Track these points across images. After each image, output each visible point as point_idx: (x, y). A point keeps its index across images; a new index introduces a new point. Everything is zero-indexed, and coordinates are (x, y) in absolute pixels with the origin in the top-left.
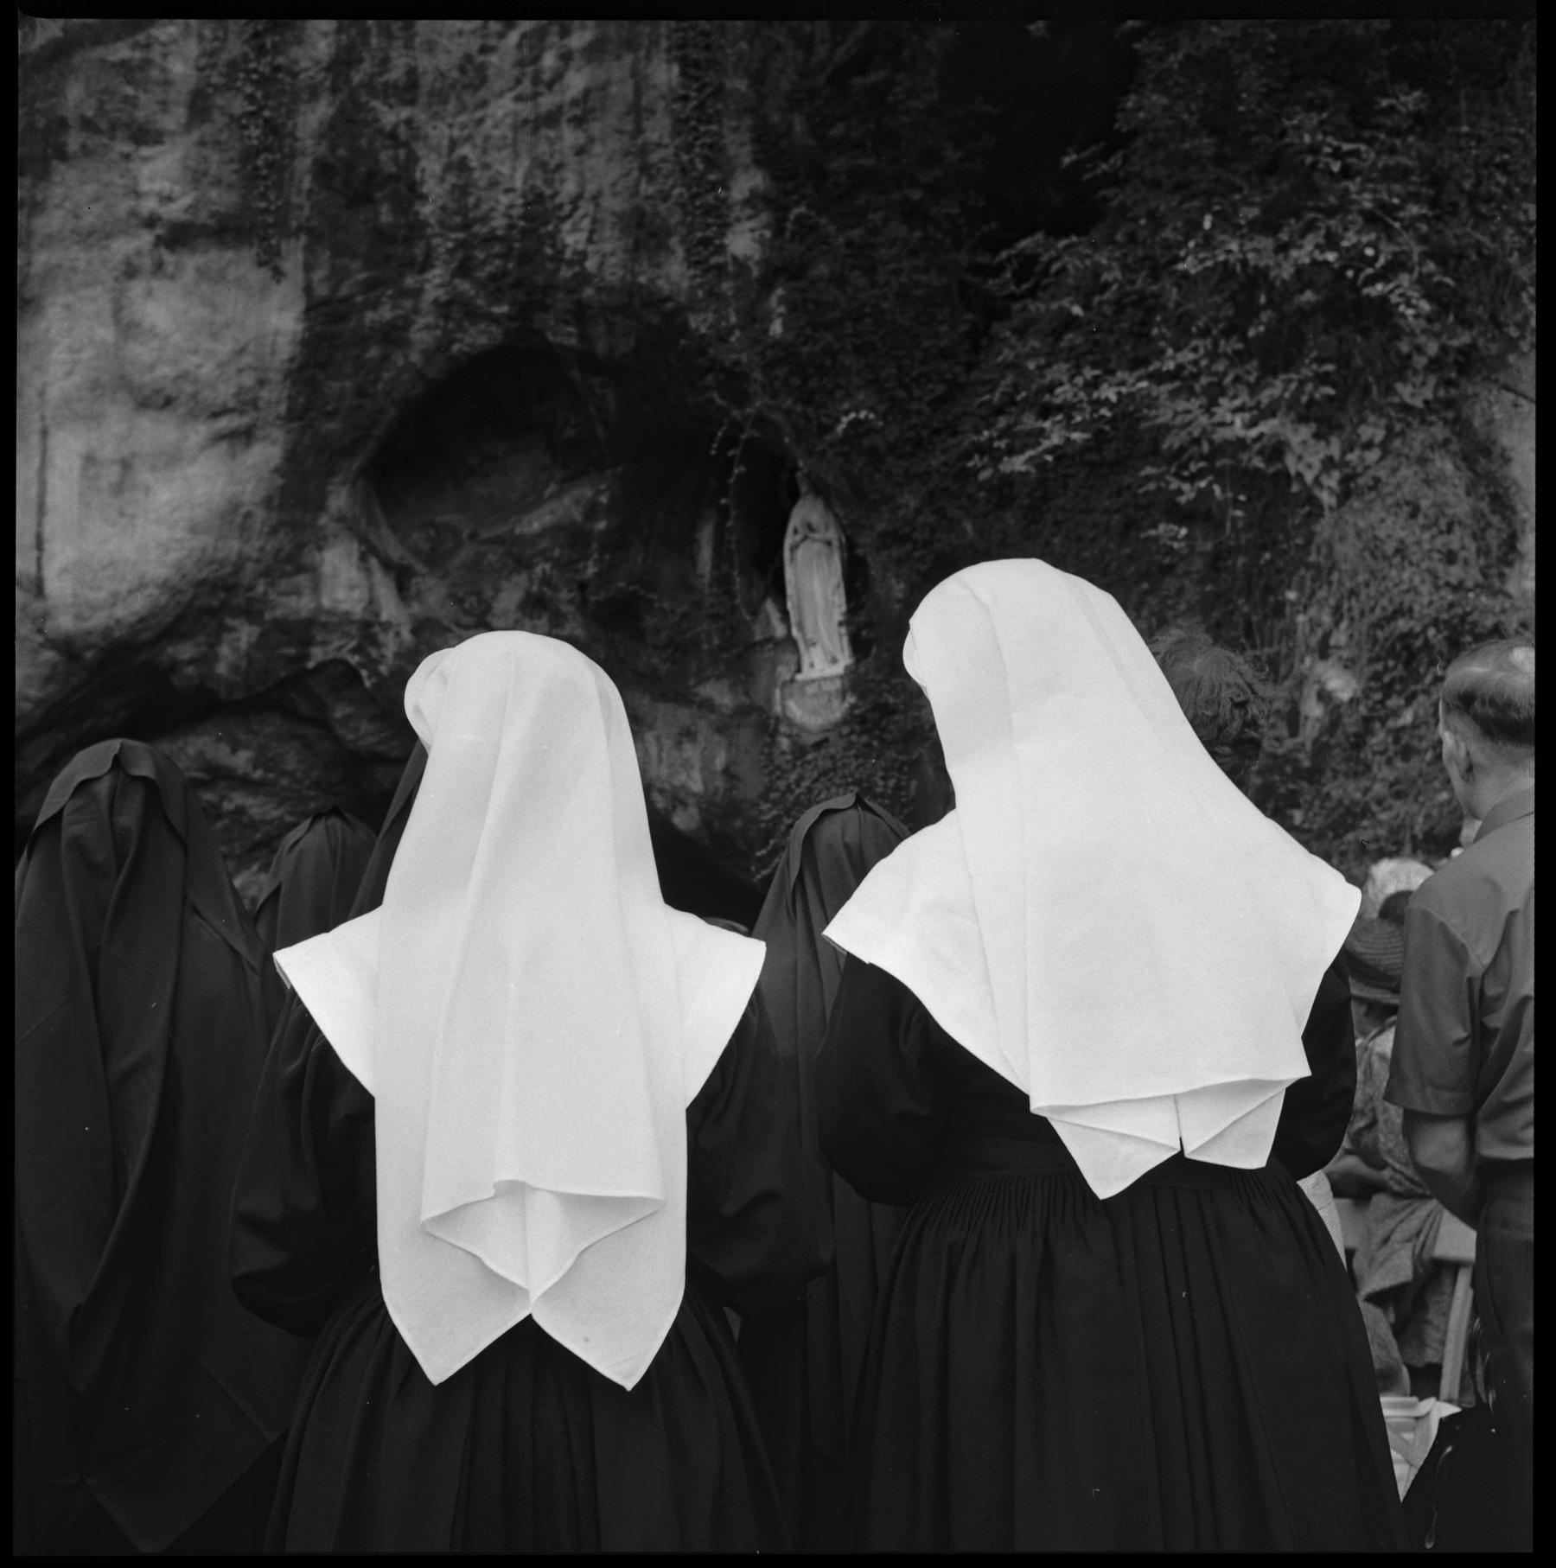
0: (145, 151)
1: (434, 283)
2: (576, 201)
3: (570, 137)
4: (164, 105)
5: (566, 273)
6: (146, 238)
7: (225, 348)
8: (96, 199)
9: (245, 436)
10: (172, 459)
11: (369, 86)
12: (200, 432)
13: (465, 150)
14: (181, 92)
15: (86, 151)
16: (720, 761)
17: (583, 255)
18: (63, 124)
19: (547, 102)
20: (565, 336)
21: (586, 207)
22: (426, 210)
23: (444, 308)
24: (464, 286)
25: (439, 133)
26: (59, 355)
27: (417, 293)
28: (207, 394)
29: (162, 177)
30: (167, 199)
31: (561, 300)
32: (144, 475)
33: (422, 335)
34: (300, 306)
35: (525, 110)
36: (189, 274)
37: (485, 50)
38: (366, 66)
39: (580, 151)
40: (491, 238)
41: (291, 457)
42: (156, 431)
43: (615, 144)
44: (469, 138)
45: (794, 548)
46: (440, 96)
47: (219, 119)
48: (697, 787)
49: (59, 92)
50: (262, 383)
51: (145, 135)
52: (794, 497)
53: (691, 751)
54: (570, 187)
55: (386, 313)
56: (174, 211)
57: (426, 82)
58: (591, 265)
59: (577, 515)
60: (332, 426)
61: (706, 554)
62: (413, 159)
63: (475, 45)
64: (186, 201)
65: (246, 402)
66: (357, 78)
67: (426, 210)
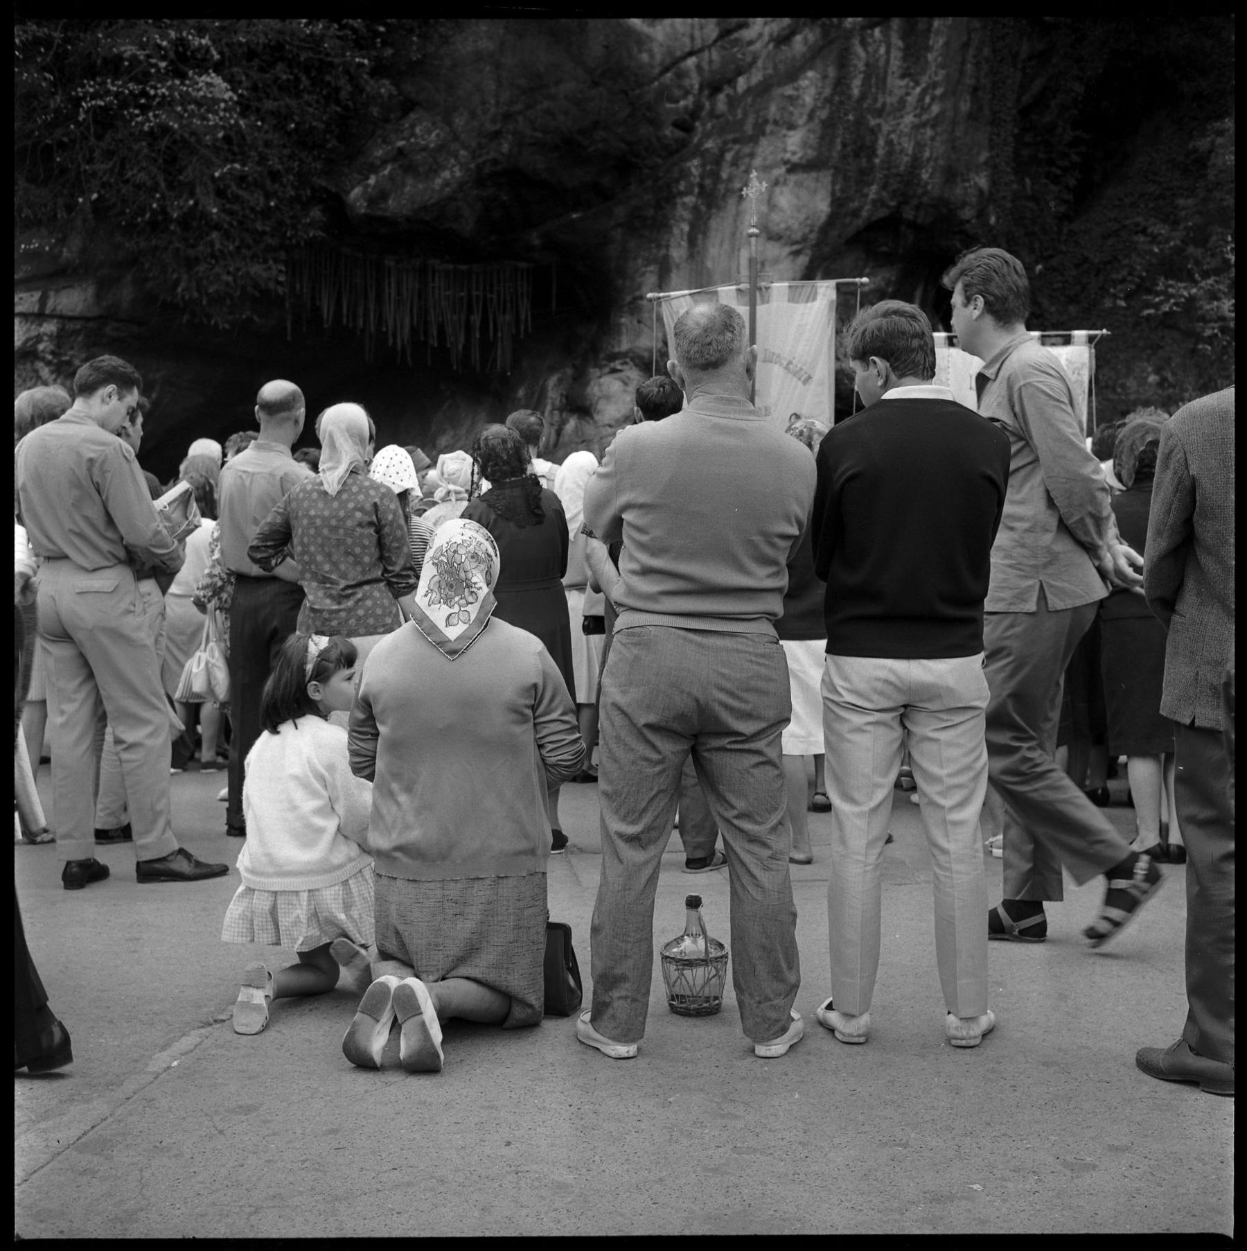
0: (791, 133)
2: (929, 160)
3: (929, 132)
4: (801, 114)
5: (920, 191)
6: (783, 169)
7: (802, 217)
8: (772, 153)
9: (796, 253)
10: (776, 261)
12: (787, 250)
13: (893, 136)
15: (772, 133)
17: (927, 183)
18: (766, 121)
19: (925, 117)
20: (908, 214)
21: (932, 163)
22: (877, 161)
23: (874, 202)
24: (884, 194)
25: (886, 128)
27: (866, 195)
28: (793, 236)
29: (795, 143)
30: (794, 153)
31: (915, 202)
32: (767, 268)
33: (864, 214)
34: (829, 200)
35: (916, 120)
36: (791, 184)
37: (908, 94)
38: (869, 101)
39: (933, 139)
41: (811, 262)
42: (773, 250)
46: (889, 114)
47: (817, 121)
49: (767, 108)
50: (811, 231)
51: (792, 127)
54: (927, 154)
55: (856, 204)
56: (795, 159)
57: (888, 108)
58: (929, 187)
59: (883, 284)
62: (876, 140)
63: (903, 91)
64: (799, 155)
65: (804, 239)
66: (865, 105)
67: (877, 161)
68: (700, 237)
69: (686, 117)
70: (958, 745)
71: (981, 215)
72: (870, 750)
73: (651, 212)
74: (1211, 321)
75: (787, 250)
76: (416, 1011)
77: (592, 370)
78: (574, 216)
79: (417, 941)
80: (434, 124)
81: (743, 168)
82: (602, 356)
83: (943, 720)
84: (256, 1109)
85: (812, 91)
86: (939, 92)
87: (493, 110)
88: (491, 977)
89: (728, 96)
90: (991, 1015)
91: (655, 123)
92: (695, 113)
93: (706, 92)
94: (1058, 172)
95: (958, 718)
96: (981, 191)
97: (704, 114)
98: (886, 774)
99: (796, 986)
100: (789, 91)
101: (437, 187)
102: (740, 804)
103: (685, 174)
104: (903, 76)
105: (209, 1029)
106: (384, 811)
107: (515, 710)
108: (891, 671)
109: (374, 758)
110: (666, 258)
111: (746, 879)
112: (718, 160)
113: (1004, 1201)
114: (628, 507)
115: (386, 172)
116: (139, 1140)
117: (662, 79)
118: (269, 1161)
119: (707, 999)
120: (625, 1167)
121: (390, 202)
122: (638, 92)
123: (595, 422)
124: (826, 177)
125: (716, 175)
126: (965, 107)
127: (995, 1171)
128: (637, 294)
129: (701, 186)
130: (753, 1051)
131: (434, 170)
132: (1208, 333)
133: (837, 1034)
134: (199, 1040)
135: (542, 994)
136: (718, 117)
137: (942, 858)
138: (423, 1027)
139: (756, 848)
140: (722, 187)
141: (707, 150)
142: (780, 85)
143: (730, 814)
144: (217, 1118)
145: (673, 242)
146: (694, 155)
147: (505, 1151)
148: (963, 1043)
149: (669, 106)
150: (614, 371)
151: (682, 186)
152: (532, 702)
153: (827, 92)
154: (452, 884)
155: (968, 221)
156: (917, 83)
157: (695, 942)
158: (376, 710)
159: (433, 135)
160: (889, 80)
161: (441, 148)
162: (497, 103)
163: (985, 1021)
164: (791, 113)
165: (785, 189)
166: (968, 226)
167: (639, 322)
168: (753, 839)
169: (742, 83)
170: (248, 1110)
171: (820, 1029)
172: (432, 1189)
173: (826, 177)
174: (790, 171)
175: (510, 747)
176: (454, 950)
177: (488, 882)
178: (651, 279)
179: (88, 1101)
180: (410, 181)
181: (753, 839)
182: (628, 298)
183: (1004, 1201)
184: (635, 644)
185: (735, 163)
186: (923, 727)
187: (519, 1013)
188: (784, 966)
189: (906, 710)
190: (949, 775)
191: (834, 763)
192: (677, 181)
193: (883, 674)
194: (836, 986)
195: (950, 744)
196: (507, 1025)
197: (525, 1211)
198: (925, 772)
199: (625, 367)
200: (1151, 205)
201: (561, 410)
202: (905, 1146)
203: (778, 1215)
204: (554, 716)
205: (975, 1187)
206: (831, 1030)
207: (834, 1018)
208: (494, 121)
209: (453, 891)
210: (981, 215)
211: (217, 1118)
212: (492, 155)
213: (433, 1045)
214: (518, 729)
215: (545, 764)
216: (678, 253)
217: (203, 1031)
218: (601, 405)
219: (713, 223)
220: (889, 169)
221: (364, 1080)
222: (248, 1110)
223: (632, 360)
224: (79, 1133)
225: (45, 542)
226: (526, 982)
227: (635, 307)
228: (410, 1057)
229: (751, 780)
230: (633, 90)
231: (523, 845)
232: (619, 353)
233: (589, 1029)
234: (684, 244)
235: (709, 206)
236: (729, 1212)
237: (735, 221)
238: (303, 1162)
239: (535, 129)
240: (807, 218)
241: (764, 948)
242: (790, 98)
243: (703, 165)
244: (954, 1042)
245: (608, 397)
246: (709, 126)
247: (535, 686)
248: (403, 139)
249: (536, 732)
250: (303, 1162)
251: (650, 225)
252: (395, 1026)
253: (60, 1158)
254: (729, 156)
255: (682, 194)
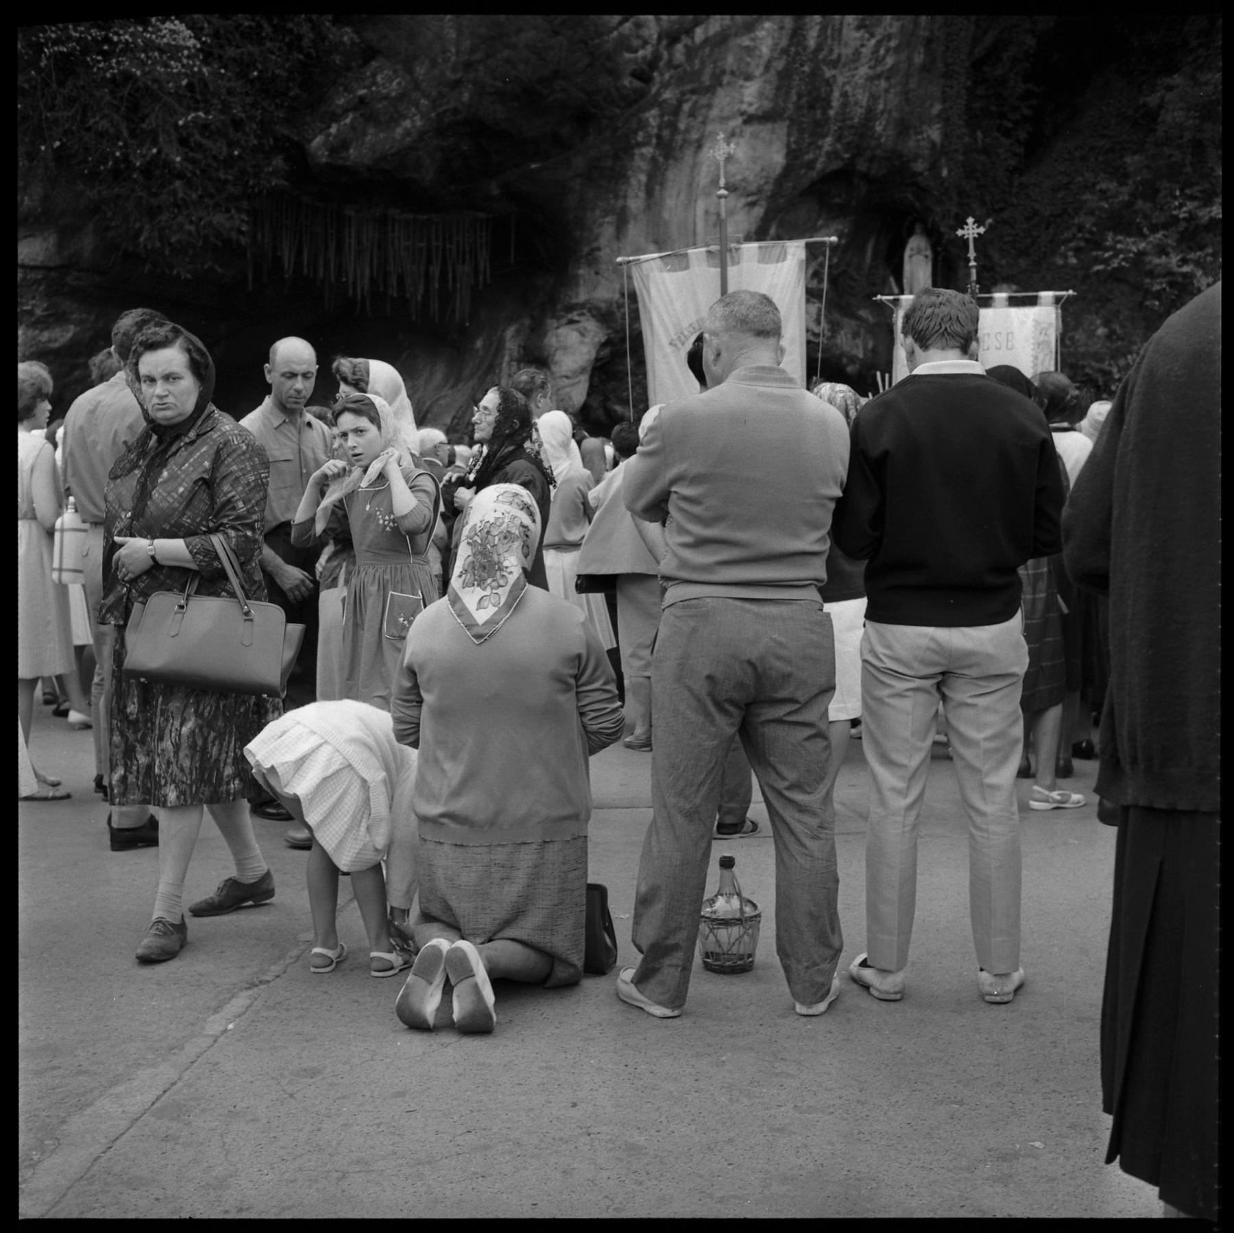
0: (748, 84)
1: (827, 143)
2: (883, 112)
3: (883, 84)
4: (758, 65)
5: (874, 143)
6: (739, 121)
7: (758, 168)
9: (752, 205)
11: (824, 61)
12: (743, 201)
13: (848, 88)
14: (763, 62)
15: (729, 84)
16: (870, 345)
18: (723, 72)
19: (879, 69)
20: (862, 166)
21: (886, 115)
23: (828, 154)
24: (839, 146)
25: (841, 80)
26: (704, 169)
27: (820, 148)
29: (751, 94)
30: (750, 104)
31: (868, 154)
33: (819, 166)
34: (784, 151)
35: (871, 72)
36: (747, 135)
37: (863, 46)
38: (825, 53)
39: (887, 91)
40: (852, 127)
41: (766, 213)
43: (898, 89)
44: (848, 83)
45: (911, 256)
46: (844, 66)
47: (773, 72)
48: (861, 355)
49: (724, 59)
50: (766, 183)
51: (749, 78)
52: (911, 233)
53: (859, 342)
54: (881, 107)
55: (811, 156)
56: (752, 110)
57: (843, 59)
58: (883, 140)
60: (782, 201)
61: (869, 254)
62: (831, 91)
63: (858, 43)
64: (755, 106)
65: (760, 191)
66: (821, 57)
68: (657, 187)
69: (645, 67)
70: (996, 711)
71: (934, 167)
72: (908, 713)
73: (609, 163)
74: (1158, 276)
75: (743, 201)
76: (470, 974)
77: (549, 321)
78: (533, 166)
79: (462, 907)
80: (395, 72)
81: (700, 119)
82: (559, 307)
83: (981, 687)
84: (320, 1072)
85: (770, 42)
86: (893, 44)
87: (453, 58)
88: (537, 939)
89: (686, 46)
90: (1021, 971)
91: (615, 73)
92: (653, 63)
93: (664, 42)
94: (1010, 125)
95: (995, 685)
96: (933, 144)
97: (662, 64)
98: (924, 739)
99: (839, 950)
100: (746, 41)
101: (398, 137)
102: (792, 776)
103: (643, 125)
104: (858, 28)
105: (256, 989)
106: (430, 778)
107: (558, 679)
108: (933, 639)
109: (418, 724)
110: (624, 209)
111: (793, 846)
112: (676, 111)
113: (1067, 1158)
114: (675, 481)
115: (348, 121)
116: (213, 1105)
117: (621, 29)
118: (345, 1125)
119: (741, 957)
120: (694, 1127)
121: (351, 151)
122: (597, 41)
123: (552, 373)
124: (782, 128)
125: (673, 126)
126: (919, 59)
127: (1053, 1128)
128: (595, 245)
129: (659, 137)
130: (794, 1008)
131: (395, 118)
132: (1157, 287)
133: (872, 990)
134: (249, 1002)
135: (583, 955)
136: (676, 67)
137: (978, 820)
138: (476, 989)
139: (805, 818)
140: (679, 138)
141: (665, 101)
142: (736, 35)
143: (781, 785)
144: (284, 1082)
145: (630, 193)
146: (651, 106)
147: (572, 1112)
148: (998, 999)
149: (628, 56)
150: (571, 322)
151: (640, 137)
152: (575, 672)
153: (784, 43)
154: (500, 849)
155: (921, 174)
156: (872, 35)
157: (728, 902)
158: (421, 679)
159: (394, 84)
160: (845, 31)
161: (402, 97)
162: (458, 52)
163: (1017, 977)
164: (748, 64)
165: (741, 140)
166: (920, 179)
167: (597, 273)
168: (801, 808)
169: (699, 34)
170: (313, 1073)
171: (855, 986)
172: (511, 1152)
173: (782, 128)
174: (746, 122)
175: (550, 712)
176: (500, 913)
177: (534, 846)
178: (608, 231)
179: (153, 1065)
180: (371, 130)
181: (801, 808)
182: (586, 250)
183: (1067, 1158)
184: (692, 617)
185: (692, 114)
186: (961, 692)
187: (561, 973)
188: (829, 931)
189: (943, 679)
190: (986, 739)
191: (872, 727)
192: (636, 133)
193: (925, 642)
194: (871, 945)
195: (987, 709)
196: (548, 984)
197: (606, 1174)
198: (961, 736)
199: (582, 318)
200: (1101, 159)
201: (519, 361)
202: (961, 1103)
203: (851, 1175)
204: (596, 685)
205: (1037, 1144)
206: (866, 987)
207: (868, 975)
208: (454, 70)
209: (500, 855)
210: (934, 167)
211: (284, 1082)
212: (452, 105)
213: (486, 1007)
214: (562, 698)
215: (587, 732)
216: (635, 203)
217: (250, 992)
218: (559, 356)
219: (671, 174)
220: (843, 121)
221: (417, 1043)
222: (313, 1073)
223: (590, 311)
224: (151, 1098)
225: (91, 508)
226: (568, 942)
227: (592, 259)
228: (464, 1018)
229: (803, 752)
230: (593, 39)
231: (567, 811)
232: (577, 304)
233: (632, 990)
234: (642, 195)
235: (667, 156)
236: (803, 1173)
237: (692, 172)
238: (379, 1125)
239: (495, 79)
240: (762, 170)
241: (811, 914)
242: (747, 48)
243: (661, 116)
244: (988, 998)
245: (565, 348)
246: (667, 76)
247: (579, 656)
248: (364, 87)
249: (578, 700)
250: (379, 1125)
251: (610, 175)
252: (448, 989)
253: (139, 1123)
254: (686, 107)
255: (640, 145)
